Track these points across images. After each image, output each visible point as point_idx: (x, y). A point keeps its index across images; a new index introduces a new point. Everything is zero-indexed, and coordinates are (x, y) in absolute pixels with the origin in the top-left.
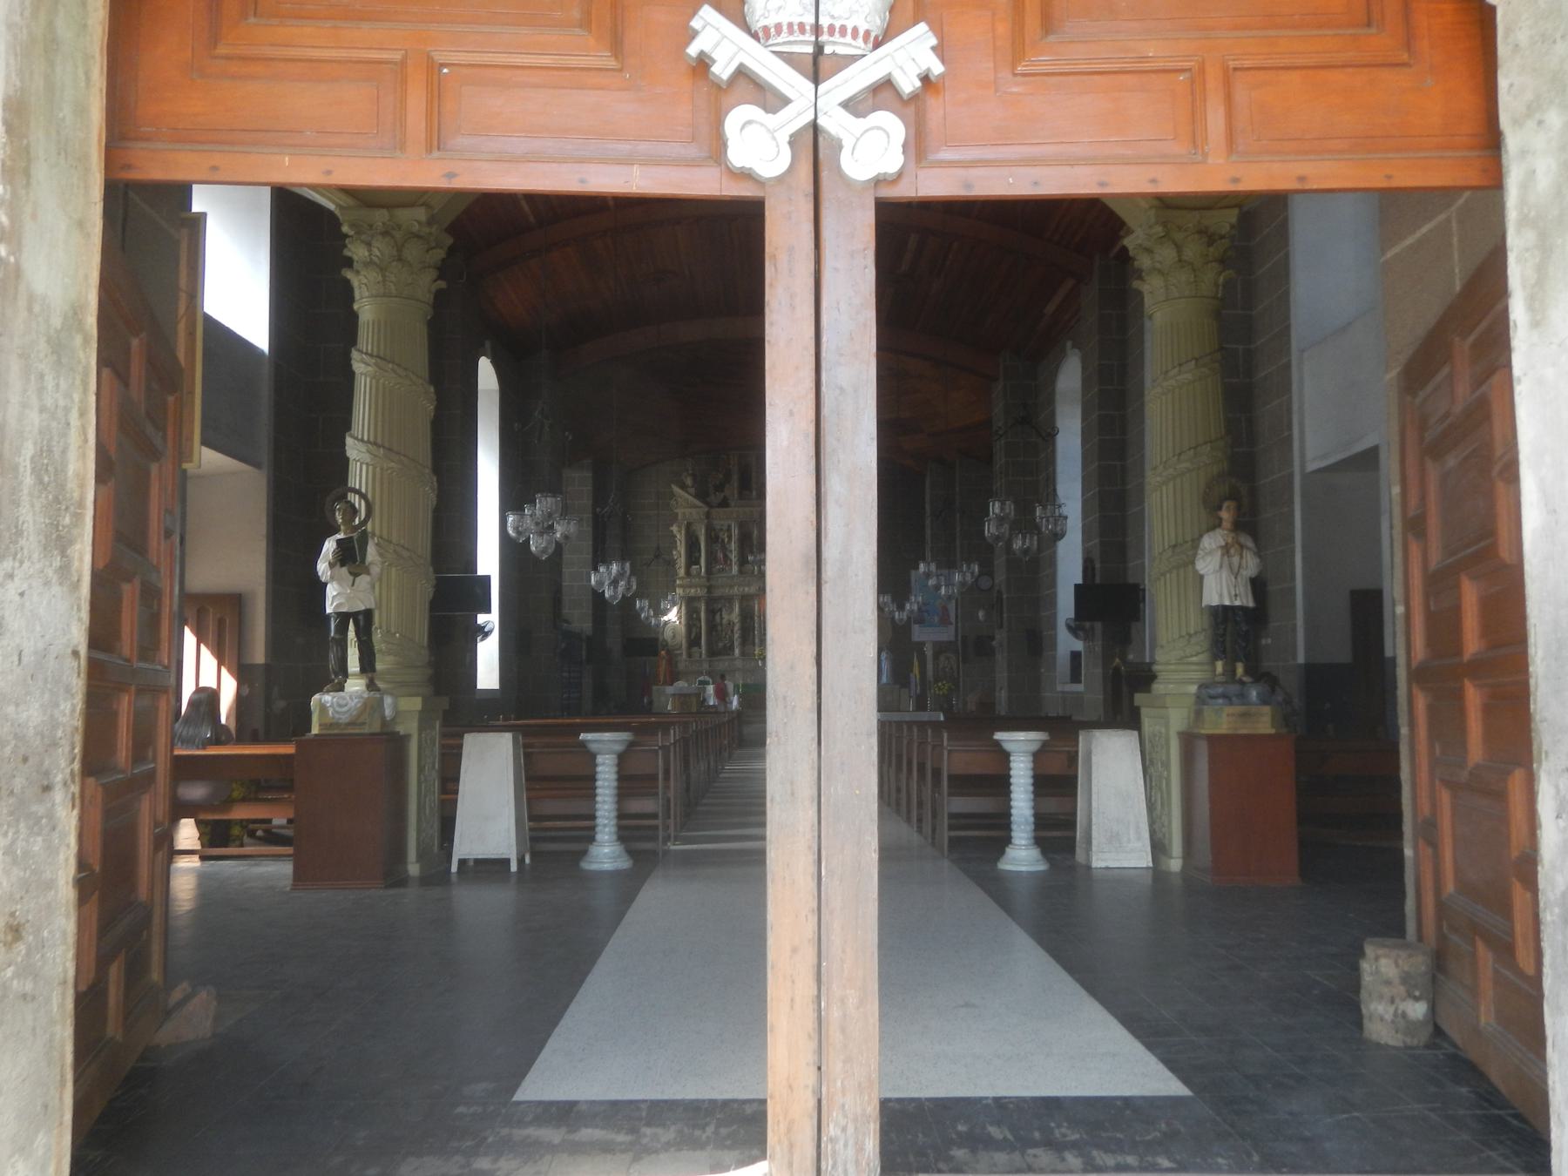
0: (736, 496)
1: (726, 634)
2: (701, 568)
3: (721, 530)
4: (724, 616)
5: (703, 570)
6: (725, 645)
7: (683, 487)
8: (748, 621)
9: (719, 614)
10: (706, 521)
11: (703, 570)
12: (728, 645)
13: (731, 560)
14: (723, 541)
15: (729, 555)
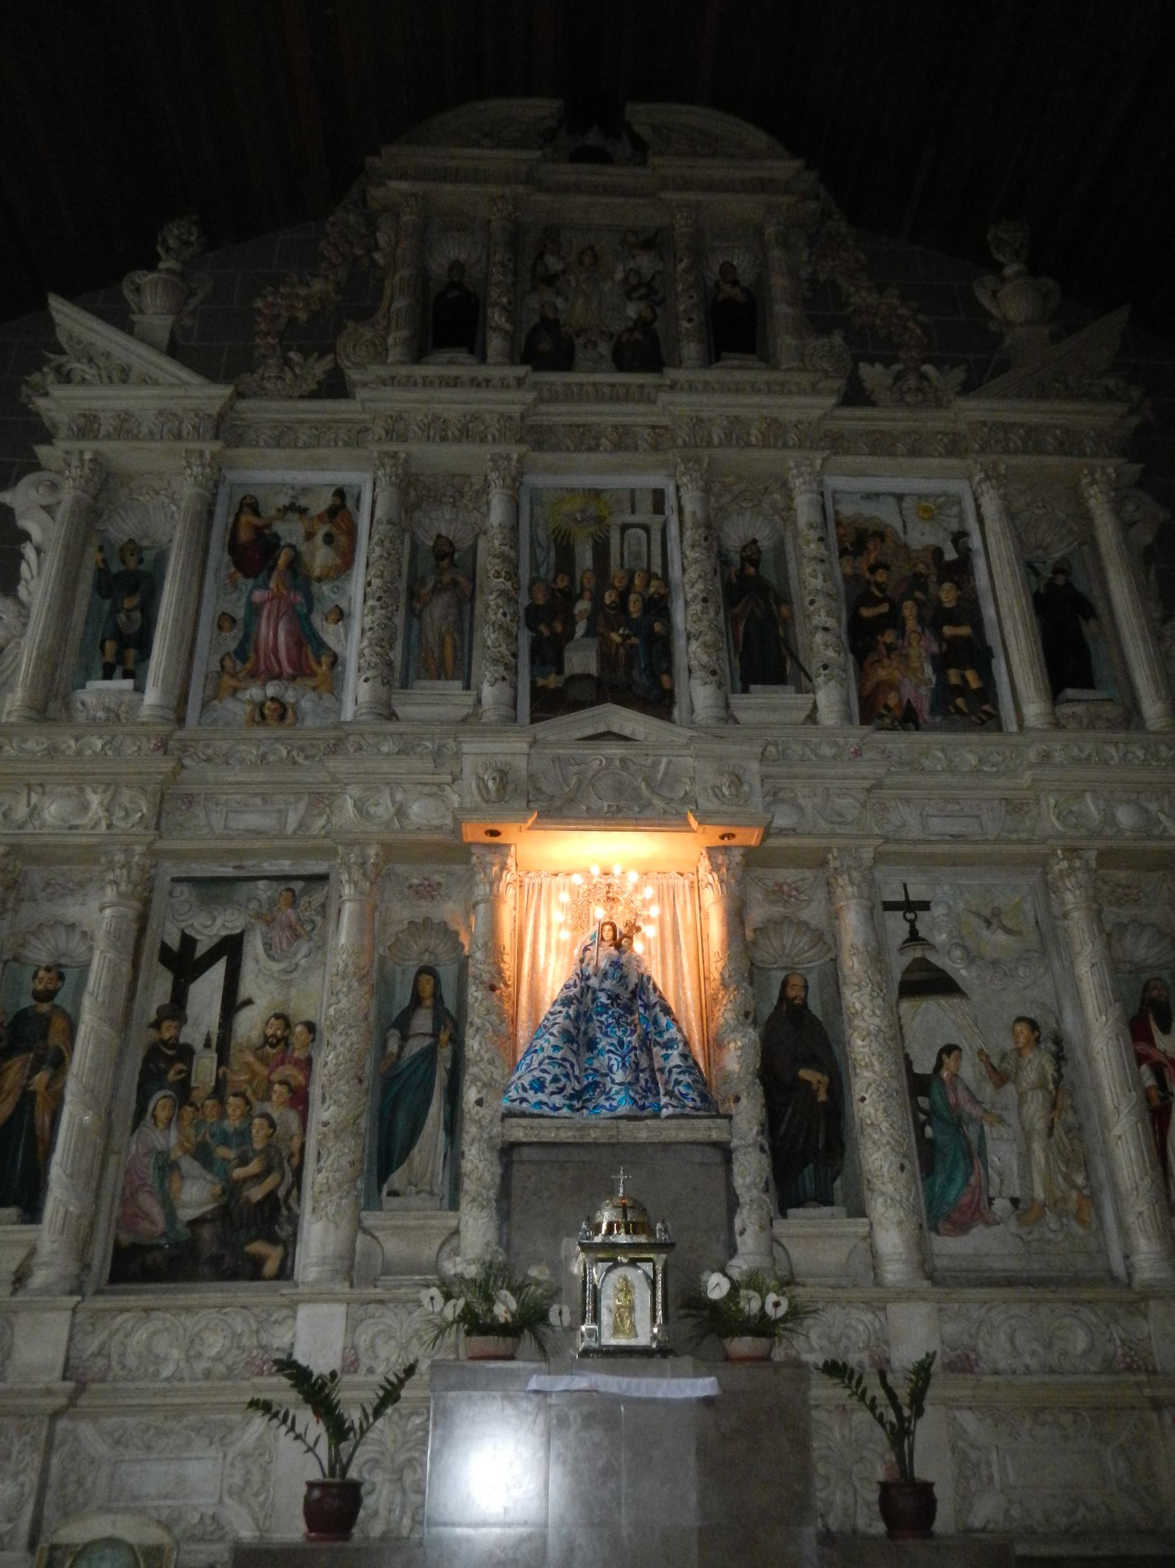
0: (394, 354)
1: (248, 1115)
2: (139, 689)
3: (303, 511)
4: (248, 986)
5: (152, 696)
6: (232, 1190)
7: (121, 319)
8: (423, 1021)
9: (217, 973)
10: (211, 447)
11: (152, 696)
12: (256, 1194)
13: (335, 660)
14: (296, 564)
15: (330, 634)
